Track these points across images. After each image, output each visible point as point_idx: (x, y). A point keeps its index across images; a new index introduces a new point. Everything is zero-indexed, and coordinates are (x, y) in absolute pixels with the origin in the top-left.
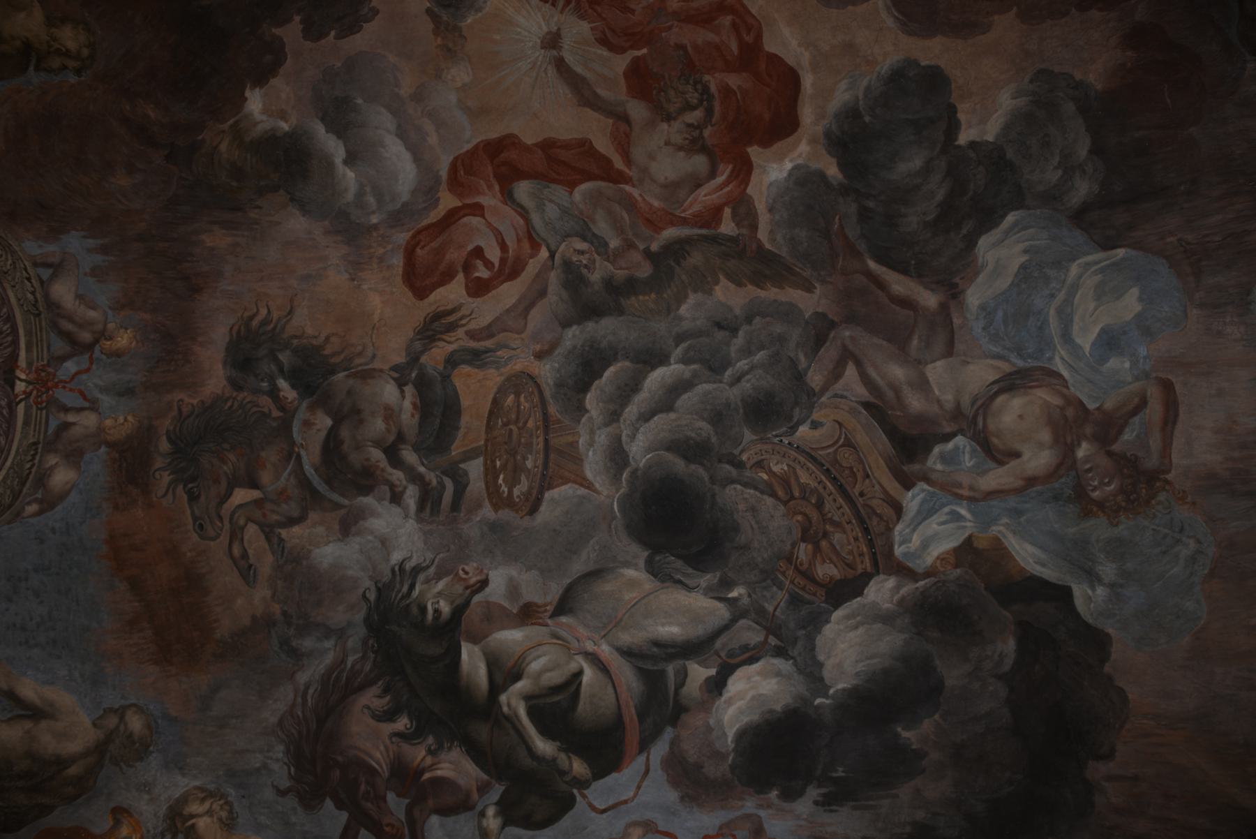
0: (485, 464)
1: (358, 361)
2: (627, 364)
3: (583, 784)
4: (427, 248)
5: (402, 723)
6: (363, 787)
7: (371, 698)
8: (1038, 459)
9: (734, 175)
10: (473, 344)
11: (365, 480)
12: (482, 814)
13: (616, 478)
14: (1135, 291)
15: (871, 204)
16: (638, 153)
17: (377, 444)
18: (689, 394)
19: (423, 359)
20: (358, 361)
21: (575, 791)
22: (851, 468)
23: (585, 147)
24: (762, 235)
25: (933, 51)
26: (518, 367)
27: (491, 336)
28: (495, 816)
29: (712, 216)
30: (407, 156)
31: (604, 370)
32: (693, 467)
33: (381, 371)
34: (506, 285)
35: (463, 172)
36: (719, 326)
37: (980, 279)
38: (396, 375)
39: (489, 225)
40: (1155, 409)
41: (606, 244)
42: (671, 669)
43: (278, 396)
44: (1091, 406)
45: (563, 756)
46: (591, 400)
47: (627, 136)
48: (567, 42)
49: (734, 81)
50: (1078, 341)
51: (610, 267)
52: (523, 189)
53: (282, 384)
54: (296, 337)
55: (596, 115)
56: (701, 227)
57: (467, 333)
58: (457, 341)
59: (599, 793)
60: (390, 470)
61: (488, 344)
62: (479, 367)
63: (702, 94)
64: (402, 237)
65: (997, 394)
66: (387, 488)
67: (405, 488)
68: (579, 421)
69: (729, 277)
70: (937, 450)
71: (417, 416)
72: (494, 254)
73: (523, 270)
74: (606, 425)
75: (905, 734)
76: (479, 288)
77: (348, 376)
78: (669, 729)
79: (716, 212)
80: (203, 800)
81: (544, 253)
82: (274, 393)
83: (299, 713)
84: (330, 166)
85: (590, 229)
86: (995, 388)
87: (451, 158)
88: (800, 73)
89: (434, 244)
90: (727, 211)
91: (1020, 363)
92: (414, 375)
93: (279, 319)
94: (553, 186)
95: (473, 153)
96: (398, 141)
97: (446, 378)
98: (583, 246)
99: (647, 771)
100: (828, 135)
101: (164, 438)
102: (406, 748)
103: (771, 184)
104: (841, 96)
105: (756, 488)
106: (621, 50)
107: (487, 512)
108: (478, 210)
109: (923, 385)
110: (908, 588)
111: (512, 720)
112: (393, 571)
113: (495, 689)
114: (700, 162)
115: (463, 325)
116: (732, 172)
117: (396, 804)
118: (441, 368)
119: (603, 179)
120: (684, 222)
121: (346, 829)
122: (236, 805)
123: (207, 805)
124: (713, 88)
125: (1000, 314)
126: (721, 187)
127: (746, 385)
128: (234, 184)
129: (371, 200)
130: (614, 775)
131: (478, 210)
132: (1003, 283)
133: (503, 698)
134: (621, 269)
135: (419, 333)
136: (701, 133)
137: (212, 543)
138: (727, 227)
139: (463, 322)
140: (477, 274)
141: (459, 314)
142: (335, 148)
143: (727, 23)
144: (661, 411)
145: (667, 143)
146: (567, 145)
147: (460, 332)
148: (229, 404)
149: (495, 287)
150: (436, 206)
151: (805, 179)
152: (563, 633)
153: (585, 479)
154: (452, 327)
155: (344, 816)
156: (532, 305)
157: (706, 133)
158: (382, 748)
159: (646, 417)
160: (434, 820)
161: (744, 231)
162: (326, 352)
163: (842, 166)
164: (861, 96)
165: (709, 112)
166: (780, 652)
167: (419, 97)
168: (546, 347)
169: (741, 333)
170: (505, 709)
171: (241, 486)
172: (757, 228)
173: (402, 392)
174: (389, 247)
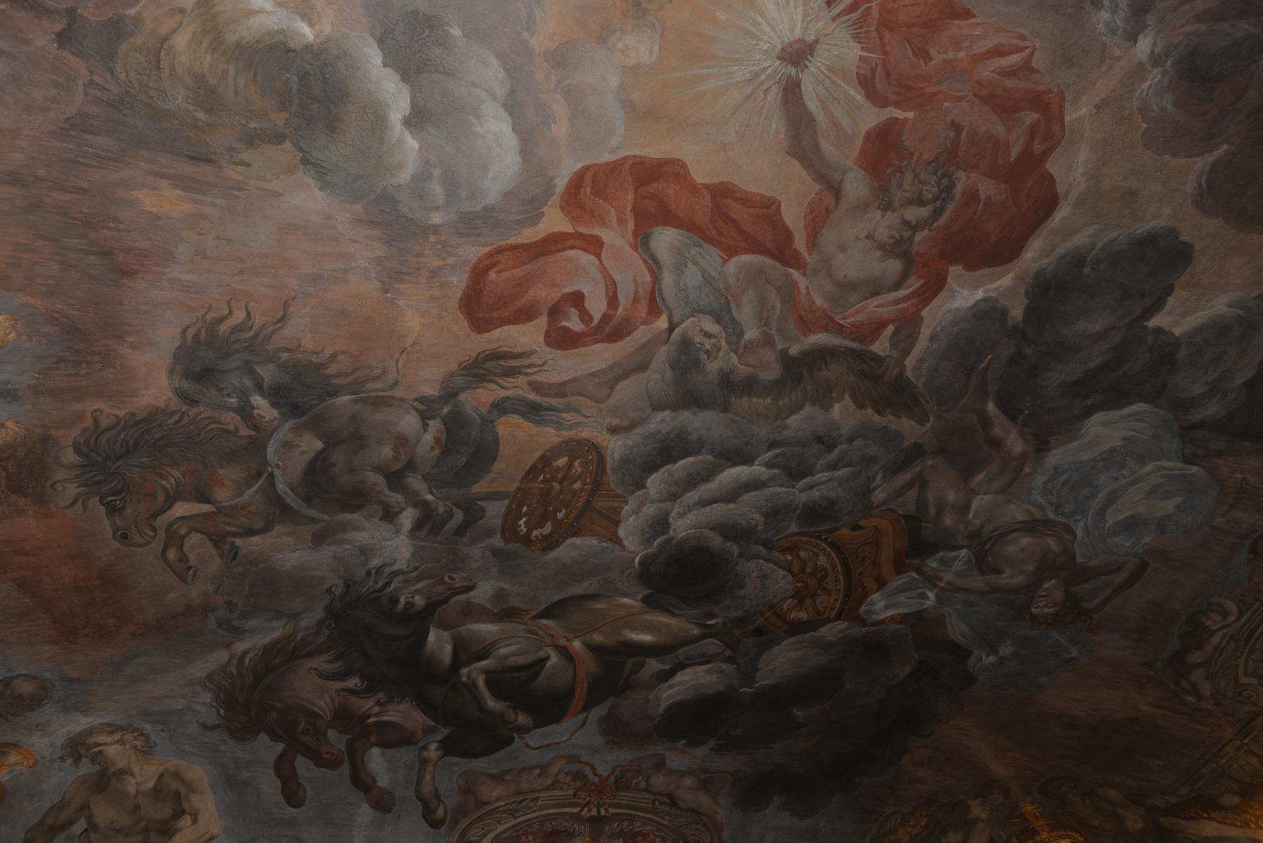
0: (509, 506)
1: (371, 385)
2: (710, 458)
3: (523, 730)
4: (505, 275)
5: (352, 682)
6: (302, 726)
7: (321, 662)
8: (1010, 578)
10: (533, 397)
11: (356, 499)
12: (425, 748)
13: (647, 541)
14: (1179, 499)
15: (1028, 351)
16: (829, 238)
17: (378, 469)
18: (758, 493)
19: (463, 397)
20: (371, 385)
21: (515, 735)
22: (864, 559)
23: (768, 209)
24: (910, 362)
25: (1201, 230)
26: (585, 434)
27: (560, 395)
28: (437, 749)
30: (511, 141)
31: (682, 458)
32: (728, 544)
33: (403, 400)
34: (599, 346)
35: (586, 191)
36: (819, 440)
37: (1074, 444)
38: (421, 407)
39: (603, 270)
40: (1123, 576)
41: (742, 333)
42: (630, 663)
43: (250, 414)
44: (1079, 560)
45: (511, 712)
46: (655, 482)
48: (817, 63)
49: (987, 188)
50: (1108, 517)
51: (735, 359)
52: (665, 239)
53: (258, 401)
54: (286, 350)
55: (804, 173)
56: (854, 340)
57: (530, 383)
58: (517, 388)
59: (536, 738)
60: (387, 492)
61: (554, 402)
62: (534, 422)
64: (473, 252)
65: (1015, 531)
66: (380, 508)
67: (403, 510)
68: (633, 493)
69: (854, 398)
70: (941, 554)
71: (437, 452)
72: (597, 306)
73: (629, 333)
74: (661, 501)
75: (799, 713)
76: (562, 340)
77: (355, 401)
78: (612, 699)
79: (882, 325)
80: (111, 733)
81: (662, 323)
82: (245, 410)
83: (234, 670)
84: (379, 120)
85: (729, 311)
86: (1019, 526)
87: (579, 166)
88: (1062, 202)
89: (517, 272)
90: (890, 329)
91: (1051, 516)
92: (445, 411)
93: (263, 326)
94: (707, 246)
95: (614, 168)
96: (503, 114)
97: (488, 423)
98: (714, 328)
99: (584, 724)
100: (1038, 275)
101: (71, 450)
102: (353, 700)
104: (1081, 240)
105: (776, 564)
106: (882, 102)
107: (497, 541)
108: (594, 245)
109: (963, 509)
110: (857, 631)
111: (472, 687)
112: (368, 573)
113: (457, 663)
114: (894, 266)
115: (527, 374)
117: (336, 740)
118: (484, 411)
120: (840, 330)
121: (282, 756)
122: (153, 737)
123: (117, 736)
124: (959, 189)
125: (1066, 476)
126: (897, 302)
127: (815, 494)
128: (201, 115)
129: (438, 189)
130: (555, 726)
131: (594, 245)
132: (1086, 456)
133: (464, 671)
135: (464, 369)
136: (913, 235)
137: (139, 550)
138: (880, 347)
139: (529, 371)
140: (565, 324)
141: (527, 361)
142: (394, 96)
143: (1028, 122)
144: (722, 501)
146: (746, 200)
147: (522, 380)
148: (176, 418)
149: (585, 345)
150: (535, 224)
151: (989, 313)
152: (541, 633)
153: (616, 535)
154: (512, 372)
155: (280, 747)
156: (625, 376)
157: (919, 236)
158: (327, 699)
159: (703, 503)
160: (375, 751)
161: (895, 353)
162: (329, 371)
163: (1029, 311)
164: (1100, 246)
165: (937, 213)
166: (730, 660)
167: (559, 59)
168: (625, 423)
169: (837, 451)
170: (464, 679)
171: (185, 499)
173: (427, 425)
174: (451, 260)
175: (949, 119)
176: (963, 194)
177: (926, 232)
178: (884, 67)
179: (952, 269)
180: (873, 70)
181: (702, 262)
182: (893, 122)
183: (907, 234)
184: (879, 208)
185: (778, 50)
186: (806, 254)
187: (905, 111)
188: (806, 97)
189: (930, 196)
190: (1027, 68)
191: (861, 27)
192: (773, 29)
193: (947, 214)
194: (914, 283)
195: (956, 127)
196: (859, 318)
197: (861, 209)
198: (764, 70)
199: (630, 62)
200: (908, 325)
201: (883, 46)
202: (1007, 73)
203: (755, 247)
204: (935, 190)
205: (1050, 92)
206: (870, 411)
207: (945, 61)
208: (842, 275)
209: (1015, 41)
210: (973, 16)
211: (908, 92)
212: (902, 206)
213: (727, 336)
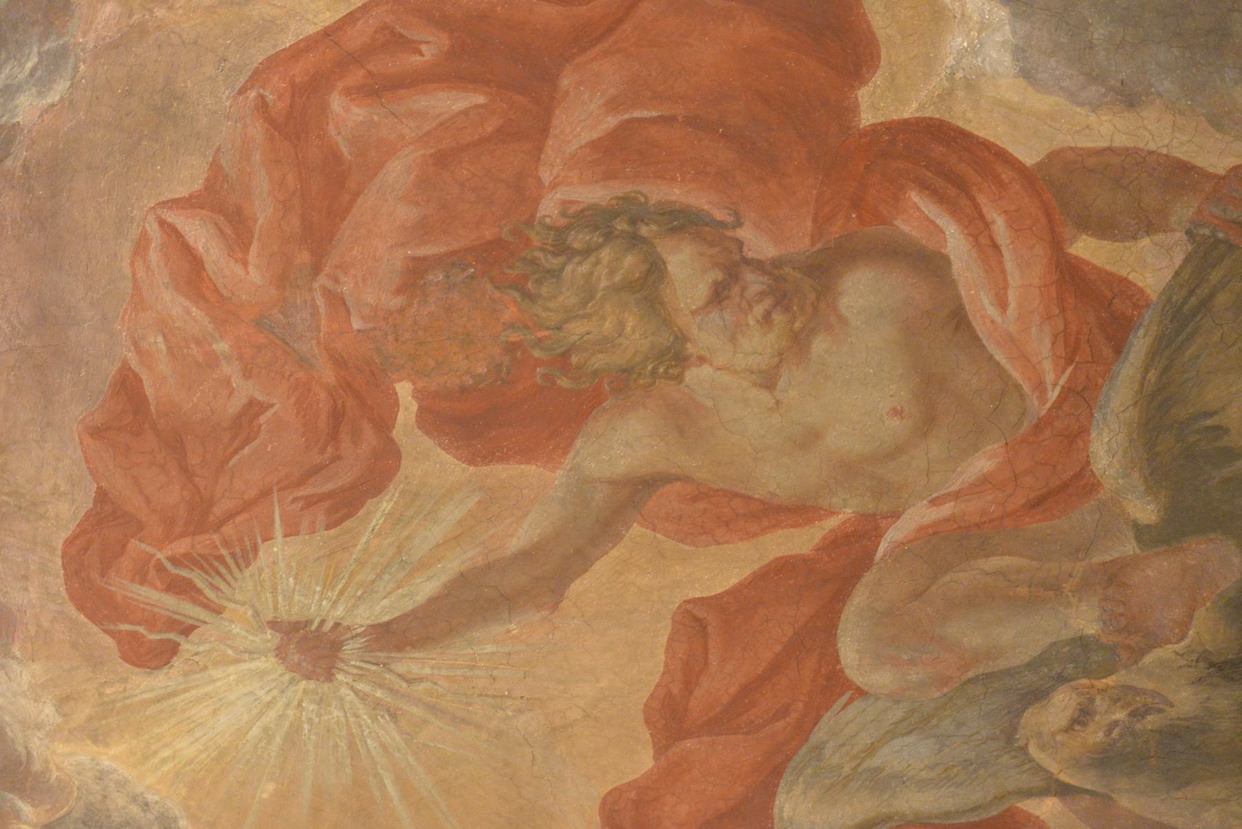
9: (954, 190)
16: (776, 479)
29: (1093, 311)
41: (1082, 643)
47: (702, 494)
49: (583, 118)
51: (1164, 653)
63: (609, 236)
79: (1072, 279)
85: (1009, 673)
90: (1087, 249)
94: (819, 734)
98: (1062, 703)
103: (1026, 74)
106: (382, 468)
114: (862, 291)
120: (1081, 396)
124: (596, 194)
126: (987, 249)
134: (1185, 625)
136: (758, 266)
138: (1148, 265)
143: (358, 113)
145: (768, 380)
146: (687, 671)
157: (758, 243)
161: (1184, 211)
165: (682, 222)
172: (1186, 168)
175: (396, 302)
176: (609, 176)
177: (745, 233)
178: (300, 483)
180: (310, 502)
181: (865, 740)
183: (755, 282)
184: (679, 378)
185: (312, 685)
186: (832, 523)
187: (396, 404)
188: (408, 605)
189: (629, 260)
191: (221, 559)
192: (269, 705)
193: (677, 193)
194: (923, 216)
195: (414, 277)
196: (1042, 346)
197: (684, 420)
198: (363, 697)
201: (247, 506)
203: (823, 628)
204: (605, 254)
205: (262, 104)
207: (247, 373)
208: (895, 423)
209: (154, 256)
210: (125, 366)
211: (350, 414)
212: (667, 322)
213: (1087, 673)
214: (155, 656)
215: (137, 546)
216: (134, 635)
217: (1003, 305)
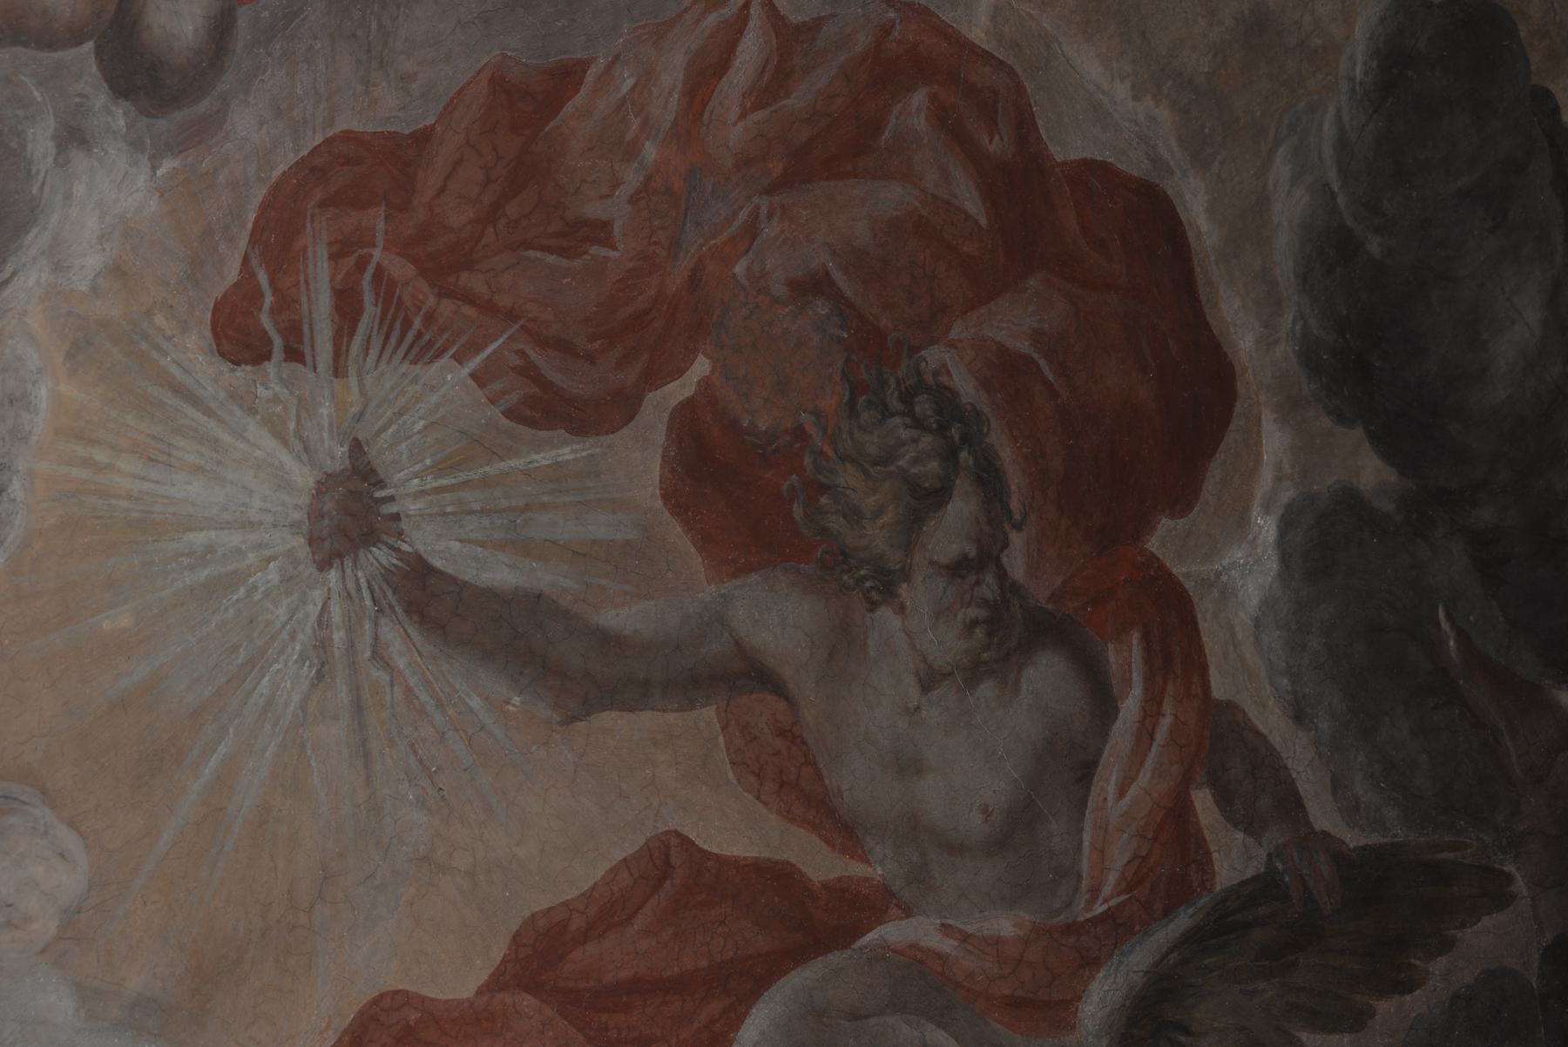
16: (857, 780)
23: (672, 875)
24: (1323, 815)
47: (790, 733)
48: (408, 487)
49: (1013, 322)
55: (647, 721)
56: (1168, 912)
63: (942, 429)
90: (1203, 801)
100: (1309, 357)
103: (1257, 623)
104: (1290, 208)
114: (1047, 677)
116: (1148, 650)
119: (797, 956)
120: (1117, 928)
124: (965, 386)
126: (1145, 733)
136: (1002, 575)
138: (1233, 858)
143: (920, 123)
146: (607, 911)
151: (1327, 540)
157: (1016, 562)
163: (1386, 442)
165: (989, 480)
175: (780, 290)
177: (1017, 539)
178: (542, 342)
179: (1153, 544)
180: (528, 371)
182: (686, 421)
183: (988, 588)
184: (873, 606)
185: (304, 552)
186: (858, 869)
187: (681, 372)
188: (469, 574)
189: (934, 466)
190: (792, 39)
191: (407, 324)
192: (248, 525)
193: (1007, 456)
194: (1127, 659)
195: (811, 286)
196: (1119, 857)
197: (842, 648)
198: (323, 620)
199: (46, 926)
200: (1219, 748)
201: (489, 308)
202: (774, 83)
203: (745, 981)
204: (927, 441)
205: (886, 30)
206: (1385, 1007)
207: (633, 200)
208: (977, 819)
210: (584, 65)
211: (644, 333)
214: (238, 339)
215: (377, 220)
216: (256, 296)
217: (1121, 794)
